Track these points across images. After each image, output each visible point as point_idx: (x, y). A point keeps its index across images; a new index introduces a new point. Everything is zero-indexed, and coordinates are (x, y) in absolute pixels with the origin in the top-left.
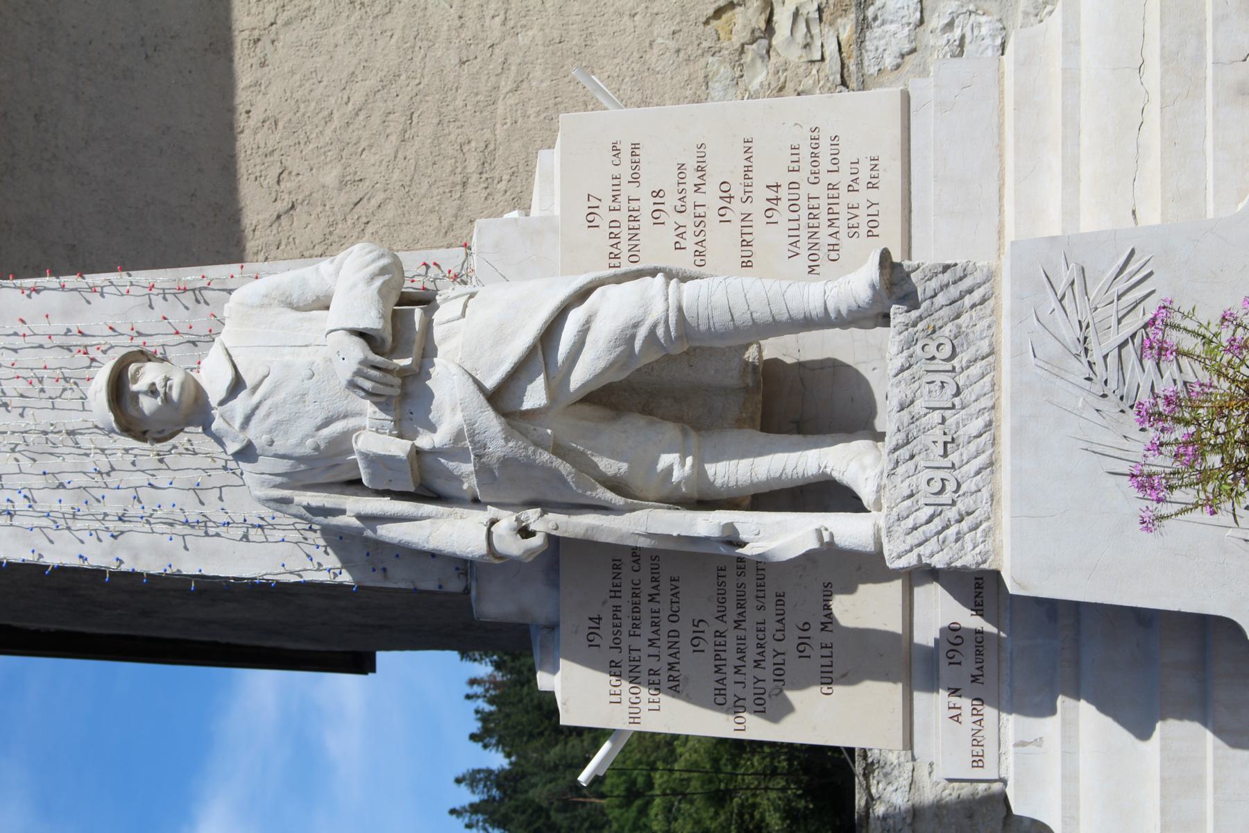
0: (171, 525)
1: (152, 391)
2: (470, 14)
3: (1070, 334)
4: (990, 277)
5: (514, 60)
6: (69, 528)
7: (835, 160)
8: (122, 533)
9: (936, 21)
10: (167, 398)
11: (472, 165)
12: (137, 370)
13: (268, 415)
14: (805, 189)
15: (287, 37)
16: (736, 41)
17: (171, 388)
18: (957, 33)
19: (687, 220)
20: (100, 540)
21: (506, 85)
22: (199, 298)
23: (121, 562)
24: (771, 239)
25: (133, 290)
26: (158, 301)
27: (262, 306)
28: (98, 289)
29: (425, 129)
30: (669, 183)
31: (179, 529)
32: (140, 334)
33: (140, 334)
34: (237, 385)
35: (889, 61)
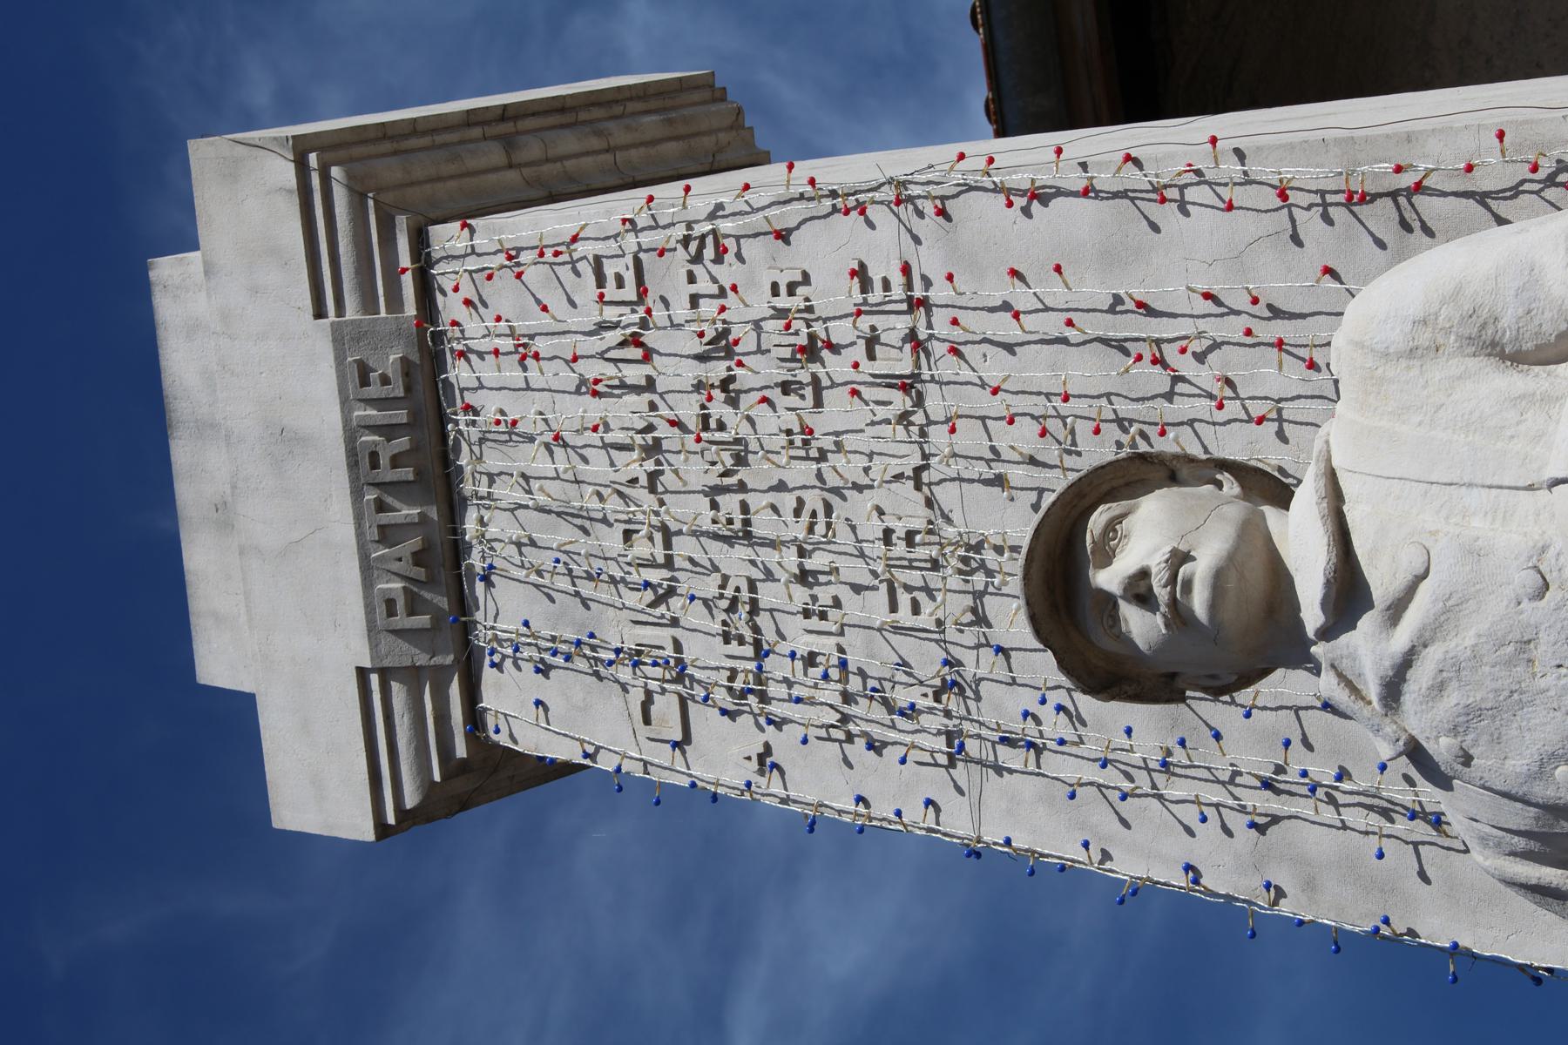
0: (1386, 814)
1: (1139, 589)
6: (1160, 797)
8: (1276, 819)
10: (1179, 615)
12: (1111, 526)
13: (1439, 687)
17: (1188, 585)
20: (1229, 833)
22: (1409, 215)
23: (1280, 893)
25: (1240, 196)
26: (1310, 223)
27: (1412, 353)
28: (1172, 193)
31: (1401, 826)
32: (1276, 313)
33: (1276, 313)
34: (1348, 593)
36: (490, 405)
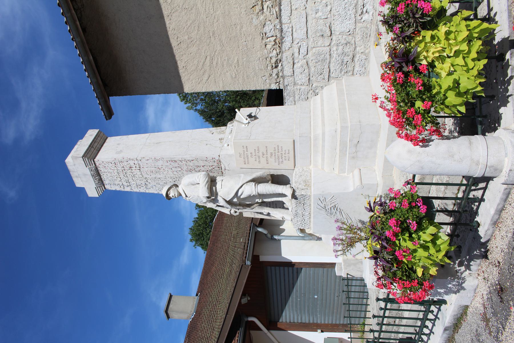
2: (207, 9)
3: (323, 206)
4: (310, 196)
5: (216, 17)
7: (282, 150)
9: (295, 43)
11: (211, 34)
14: (277, 154)
15: (174, 15)
16: (257, 11)
18: (299, 44)
19: (257, 157)
21: (215, 21)
24: (272, 160)
29: (202, 29)
30: (253, 152)
35: (287, 49)
36: (103, 170)
